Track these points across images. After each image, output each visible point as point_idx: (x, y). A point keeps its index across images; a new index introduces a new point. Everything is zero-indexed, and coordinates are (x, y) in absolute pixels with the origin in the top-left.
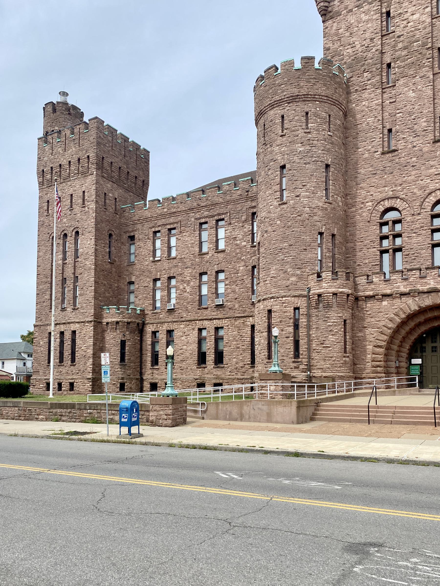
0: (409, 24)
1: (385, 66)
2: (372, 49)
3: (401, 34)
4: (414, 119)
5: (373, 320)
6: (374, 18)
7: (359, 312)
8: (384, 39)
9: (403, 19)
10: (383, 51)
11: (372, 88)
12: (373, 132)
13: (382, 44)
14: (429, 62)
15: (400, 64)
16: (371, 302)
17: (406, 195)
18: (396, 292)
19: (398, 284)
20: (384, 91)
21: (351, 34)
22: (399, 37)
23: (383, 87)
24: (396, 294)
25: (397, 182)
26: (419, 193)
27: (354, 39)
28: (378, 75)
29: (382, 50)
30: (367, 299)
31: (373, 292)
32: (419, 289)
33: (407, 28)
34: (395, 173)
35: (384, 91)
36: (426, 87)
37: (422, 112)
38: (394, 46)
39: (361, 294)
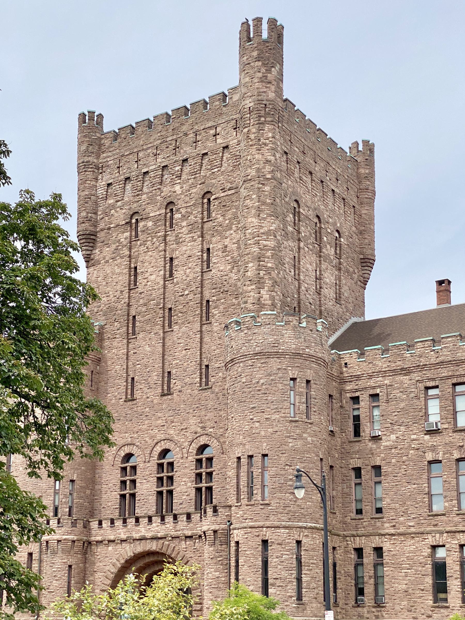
0: (149, 283)
1: (131, 318)
2: (121, 301)
3: (142, 291)
4: (149, 372)
5: (101, 564)
6: (124, 272)
7: (92, 556)
8: (131, 292)
9: (144, 277)
10: (131, 304)
11: (120, 338)
12: (119, 379)
13: (129, 297)
14: (161, 321)
15: (141, 319)
16: (101, 547)
17: (141, 443)
18: (117, 538)
19: (120, 530)
20: (130, 341)
21: (107, 283)
22: (141, 293)
23: (129, 338)
24: (118, 540)
25: (135, 429)
26: (150, 441)
27: (109, 289)
28: (125, 326)
29: (129, 303)
30: (98, 543)
31: (101, 537)
32: (133, 537)
33: (147, 287)
34: (133, 421)
35: (130, 341)
36: (158, 343)
37: (154, 366)
38: (138, 301)
39: (93, 538)
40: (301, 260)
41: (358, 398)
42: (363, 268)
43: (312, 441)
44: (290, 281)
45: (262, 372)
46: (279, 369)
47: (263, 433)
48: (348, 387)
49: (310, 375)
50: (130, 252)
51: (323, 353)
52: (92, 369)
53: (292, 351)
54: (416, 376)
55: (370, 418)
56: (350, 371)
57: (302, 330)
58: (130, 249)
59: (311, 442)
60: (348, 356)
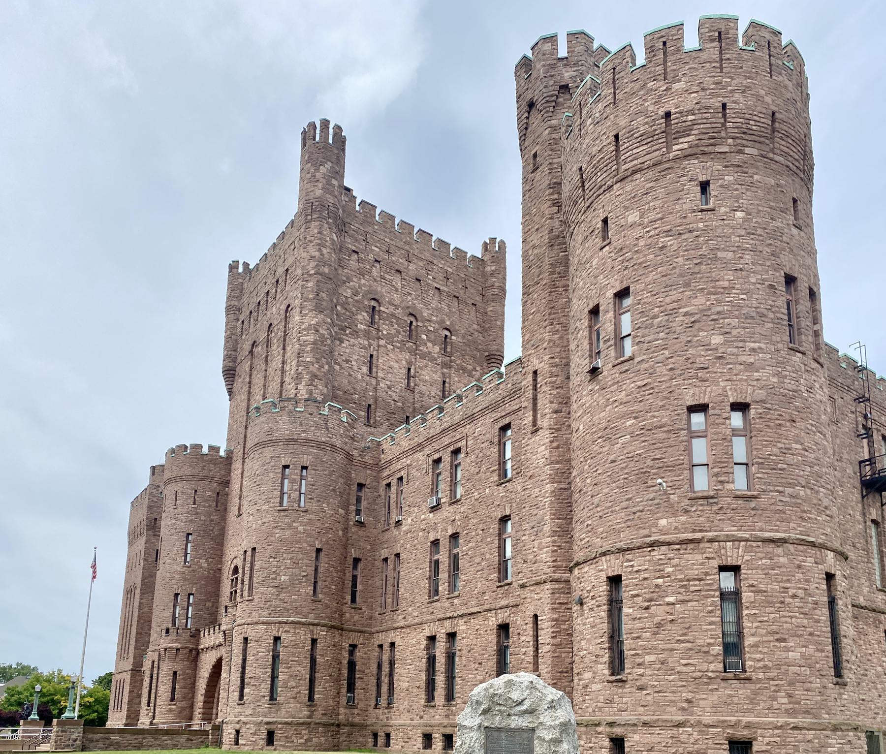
40: (380, 357)
41: (390, 483)
42: (489, 366)
43: (304, 530)
44: (359, 377)
45: (259, 463)
46: (272, 457)
47: (254, 526)
48: (386, 473)
49: (306, 460)
50: (250, 378)
51: (329, 437)
52: (218, 491)
53: (286, 438)
54: (427, 451)
55: (397, 504)
56: (385, 457)
57: (299, 415)
58: (250, 376)
59: (302, 531)
60: (385, 441)
